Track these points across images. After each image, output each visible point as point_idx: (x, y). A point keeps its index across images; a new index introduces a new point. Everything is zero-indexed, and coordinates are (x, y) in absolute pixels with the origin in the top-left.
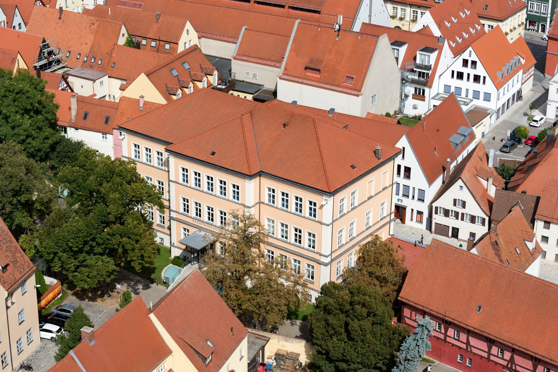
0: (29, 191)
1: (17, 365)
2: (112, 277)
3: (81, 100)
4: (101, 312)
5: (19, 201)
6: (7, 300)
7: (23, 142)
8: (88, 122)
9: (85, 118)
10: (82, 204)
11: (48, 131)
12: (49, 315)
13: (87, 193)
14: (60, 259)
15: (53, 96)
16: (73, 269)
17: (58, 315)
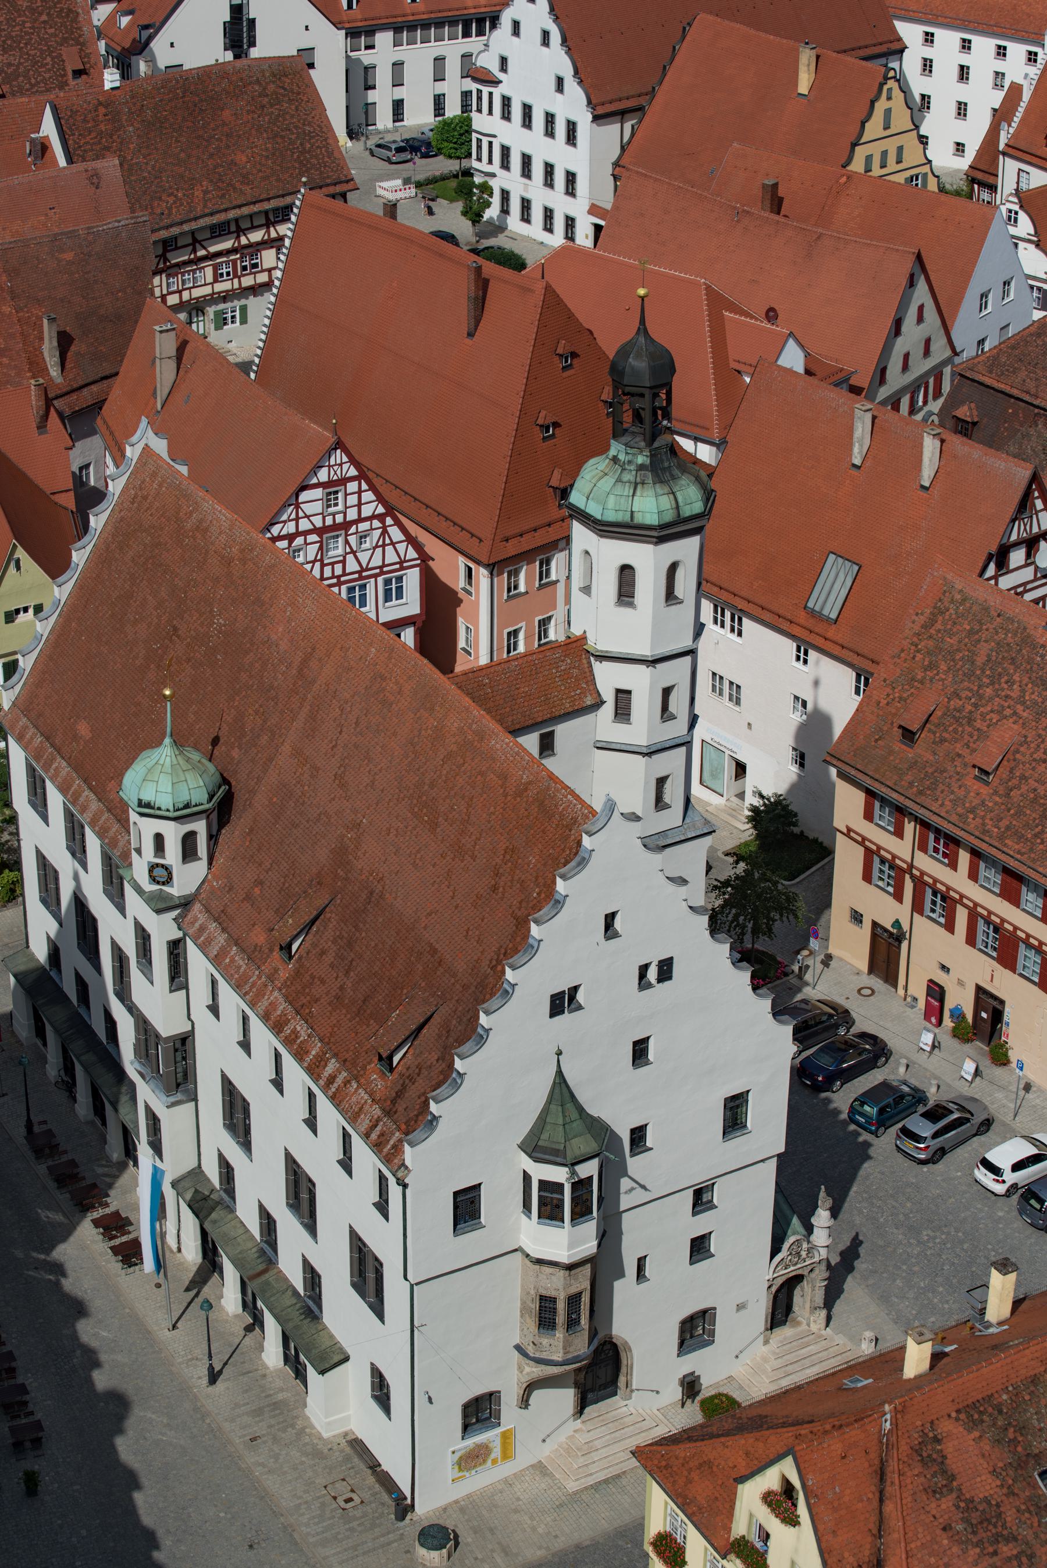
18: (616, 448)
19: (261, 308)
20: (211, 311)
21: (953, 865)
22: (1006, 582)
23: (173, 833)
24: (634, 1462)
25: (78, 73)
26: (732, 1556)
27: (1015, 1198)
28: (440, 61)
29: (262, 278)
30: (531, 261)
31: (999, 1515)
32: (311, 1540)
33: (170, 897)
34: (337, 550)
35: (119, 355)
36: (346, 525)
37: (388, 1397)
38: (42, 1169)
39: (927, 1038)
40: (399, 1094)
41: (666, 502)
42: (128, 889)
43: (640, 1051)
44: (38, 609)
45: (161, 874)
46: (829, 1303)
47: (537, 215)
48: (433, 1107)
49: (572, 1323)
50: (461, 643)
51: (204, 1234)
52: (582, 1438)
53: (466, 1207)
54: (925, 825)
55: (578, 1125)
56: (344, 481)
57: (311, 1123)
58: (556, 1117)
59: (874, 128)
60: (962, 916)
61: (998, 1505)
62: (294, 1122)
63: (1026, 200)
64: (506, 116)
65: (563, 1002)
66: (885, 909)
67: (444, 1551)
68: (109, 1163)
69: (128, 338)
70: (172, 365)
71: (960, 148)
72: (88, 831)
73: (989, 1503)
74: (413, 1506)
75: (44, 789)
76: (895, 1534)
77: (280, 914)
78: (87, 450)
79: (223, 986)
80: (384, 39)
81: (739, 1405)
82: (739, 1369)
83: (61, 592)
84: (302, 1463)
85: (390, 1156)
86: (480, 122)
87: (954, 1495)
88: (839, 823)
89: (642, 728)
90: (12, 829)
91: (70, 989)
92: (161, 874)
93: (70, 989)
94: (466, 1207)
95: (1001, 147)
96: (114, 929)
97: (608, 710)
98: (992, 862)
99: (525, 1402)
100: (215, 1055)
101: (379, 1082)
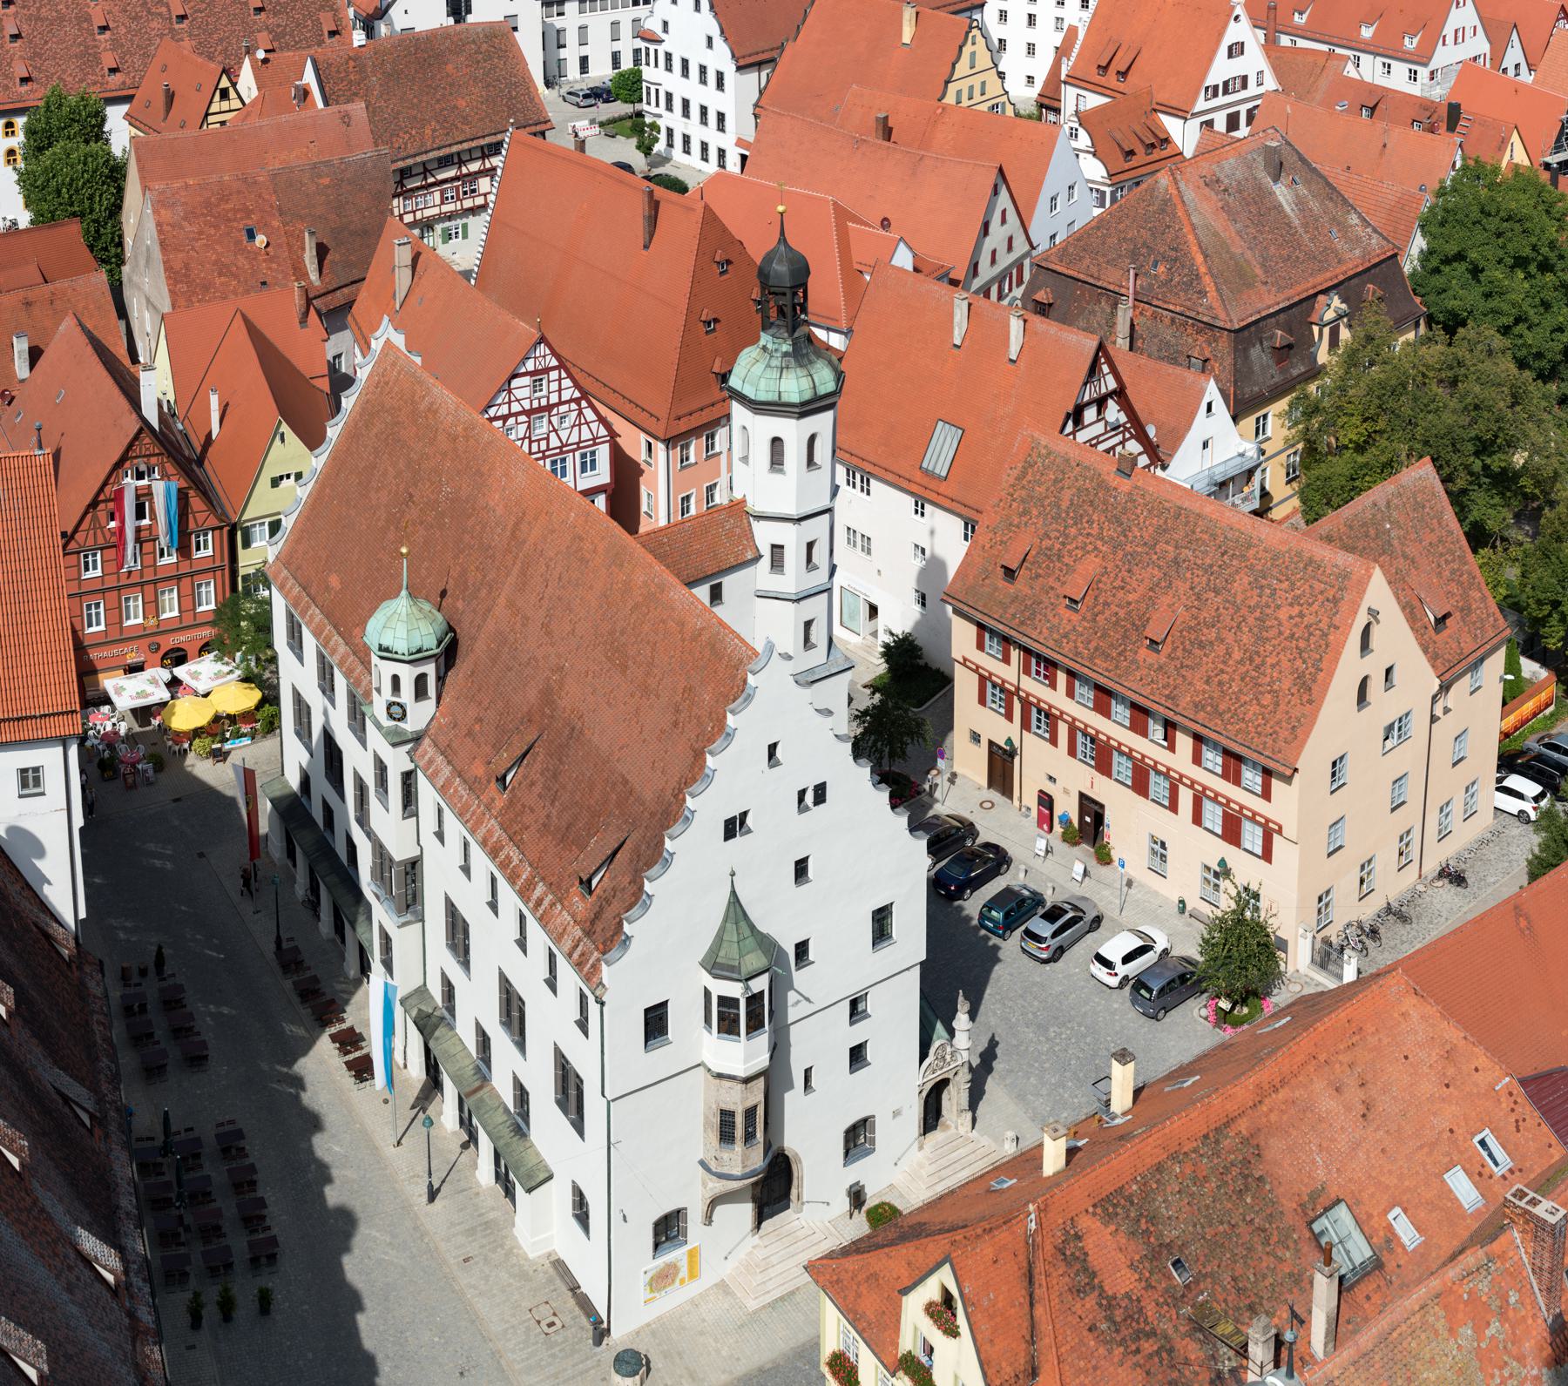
24: (807, 1278)
26: (900, 1374)
27: (1128, 989)
29: (480, 201)
31: (1141, 1310)
32: (517, 1367)
33: (404, 732)
35: (366, 263)
37: (587, 1215)
42: (369, 724)
46: (973, 1105)
48: (627, 928)
50: (644, 508)
51: (427, 1051)
52: (760, 1254)
61: (1138, 1300)
63: (1083, 118)
67: (637, 1377)
68: (347, 980)
69: (371, 249)
70: (409, 272)
72: (336, 671)
73: (1130, 1298)
74: (609, 1330)
75: (300, 633)
76: (1046, 1341)
77: (497, 747)
78: (341, 342)
81: (900, 1213)
82: (898, 1177)
84: (510, 1285)
87: (1096, 1293)
89: (792, 578)
90: (273, 667)
95: (1063, 77)
97: (766, 562)
99: (709, 1219)
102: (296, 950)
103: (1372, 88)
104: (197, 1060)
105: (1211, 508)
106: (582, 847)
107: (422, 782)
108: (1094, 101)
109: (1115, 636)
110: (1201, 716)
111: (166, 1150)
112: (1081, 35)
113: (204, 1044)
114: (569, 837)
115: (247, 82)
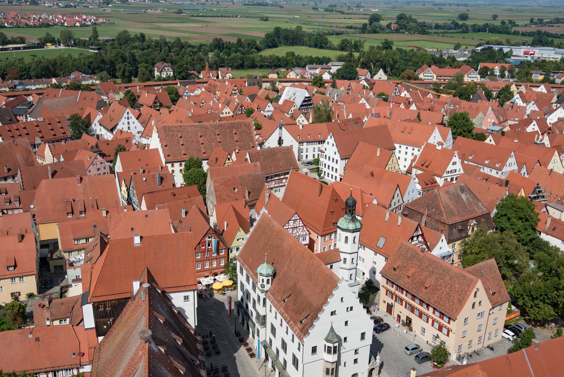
0: (514, 258)
1: (486, 345)
2: (552, 318)
3: (553, 220)
4: (543, 335)
5: (507, 263)
6: (490, 310)
7: (515, 233)
8: (555, 233)
9: (554, 229)
10: (544, 275)
11: (531, 231)
12: (510, 326)
13: (548, 269)
14: (523, 299)
15: (538, 214)
16: (530, 306)
17: (514, 327)
18: (346, 216)
19: (283, 190)
20: (274, 189)
21: (403, 293)
22: (413, 243)
23: (265, 279)
25: (253, 147)
28: (314, 148)
30: (329, 184)
34: (295, 231)
35: (259, 196)
36: (297, 227)
38: (237, 339)
39: (397, 325)
40: (303, 328)
41: (354, 226)
43: (346, 323)
44: (243, 239)
45: (263, 286)
47: (330, 176)
49: (332, 374)
53: (314, 350)
54: (397, 286)
55: (335, 336)
56: (297, 220)
57: (287, 333)
58: (331, 334)
59: (390, 162)
60: (404, 303)
62: (284, 332)
63: (417, 176)
64: (326, 158)
65: (333, 313)
66: (390, 301)
69: (260, 193)
71: (405, 166)
77: (283, 294)
78: (253, 213)
79: (272, 307)
80: (305, 144)
83: (248, 236)
85: (301, 339)
86: (321, 159)
88: (381, 284)
89: (348, 265)
91: (245, 306)
92: (263, 286)
93: (245, 306)
94: (314, 350)
96: (253, 295)
97: (342, 261)
98: (410, 293)
100: (270, 319)
101: (300, 326)
102: (239, 332)
103: (484, 174)
104: (218, 353)
105: (441, 261)
106: (301, 315)
107: (267, 300)
108: (420, 172)
109: (417, 285)
110: (435, 304)
111: (211, 370)
112: (418, 157)
113: (220, 350)
114: (298, 312)
115: (234, 157)
